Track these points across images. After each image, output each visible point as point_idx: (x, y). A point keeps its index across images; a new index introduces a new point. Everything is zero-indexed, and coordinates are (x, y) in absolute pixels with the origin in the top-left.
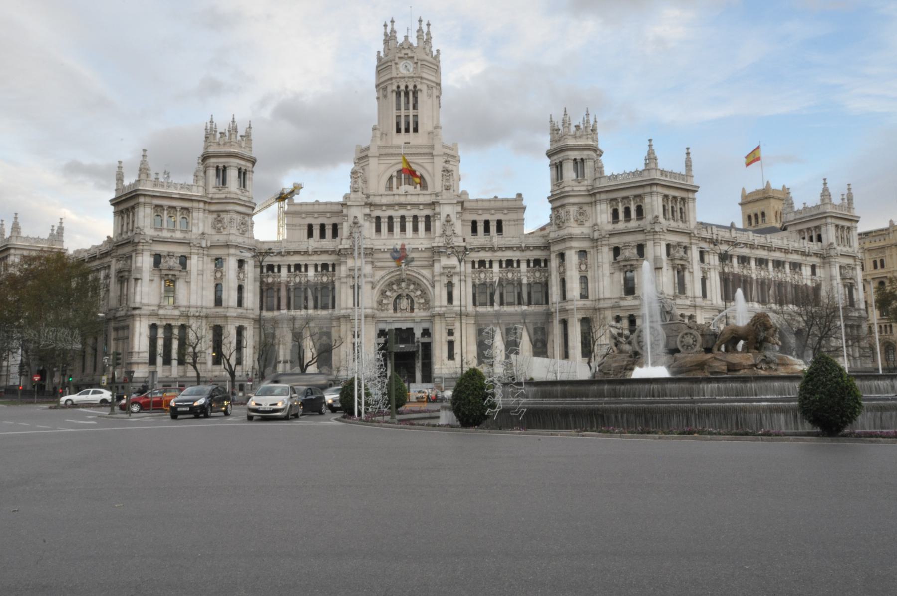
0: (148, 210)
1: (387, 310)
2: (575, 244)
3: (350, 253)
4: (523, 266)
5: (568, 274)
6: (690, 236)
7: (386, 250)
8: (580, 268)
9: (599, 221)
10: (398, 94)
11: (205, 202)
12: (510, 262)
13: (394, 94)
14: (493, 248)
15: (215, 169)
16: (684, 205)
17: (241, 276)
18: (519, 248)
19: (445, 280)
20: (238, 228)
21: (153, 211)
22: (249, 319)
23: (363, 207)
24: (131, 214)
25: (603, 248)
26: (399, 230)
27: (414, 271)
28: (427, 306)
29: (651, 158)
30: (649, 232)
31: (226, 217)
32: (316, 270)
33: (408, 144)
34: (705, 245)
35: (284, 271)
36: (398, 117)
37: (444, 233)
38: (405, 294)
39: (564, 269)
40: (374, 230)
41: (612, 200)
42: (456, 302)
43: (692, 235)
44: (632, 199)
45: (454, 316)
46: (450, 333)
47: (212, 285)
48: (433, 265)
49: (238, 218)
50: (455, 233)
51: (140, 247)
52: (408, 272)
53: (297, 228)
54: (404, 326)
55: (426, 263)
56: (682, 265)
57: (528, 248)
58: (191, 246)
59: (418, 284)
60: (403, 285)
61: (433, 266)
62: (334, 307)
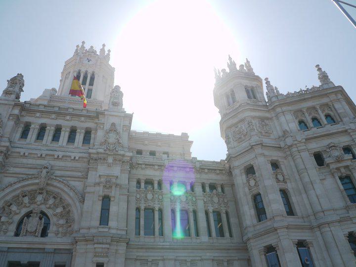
1: (5, 233)
7: (26, 154)
8: (277, 178)
19: (101, 191)
23: (11, 107)
25: (301, 154)
28: (69, 229)
29: (324, 77)
40: (18, 135)
42: (112, 223)
45: (109, 241)
52: (49, 182)
55: (79, 174)
59: (61, 198)
60: (39, 198)
61: (87, 178)
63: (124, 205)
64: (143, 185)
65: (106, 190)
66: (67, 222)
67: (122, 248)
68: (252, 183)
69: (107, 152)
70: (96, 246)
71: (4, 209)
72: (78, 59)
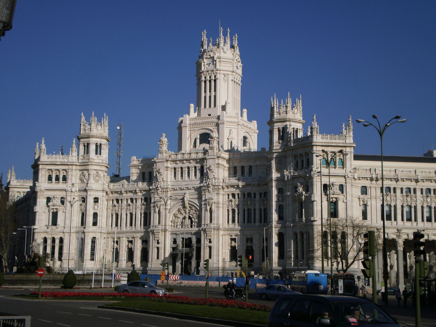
4: (258, 197)
6: (345, 178)
10: (205, 82)
11: (76, 165)
12: (249, 194)
17: (96, 207)
18: (254, 185)
20: (94, 179)
27: (191, 201)
34: (367, 183)
35: (125, 202)
36: (205, 97)
38: (187, 216)
43: (346, 177)
46: (210, 242)
49: (95, 172)
51: (39, 194)
54: (186, 236)
56: (336, 198)
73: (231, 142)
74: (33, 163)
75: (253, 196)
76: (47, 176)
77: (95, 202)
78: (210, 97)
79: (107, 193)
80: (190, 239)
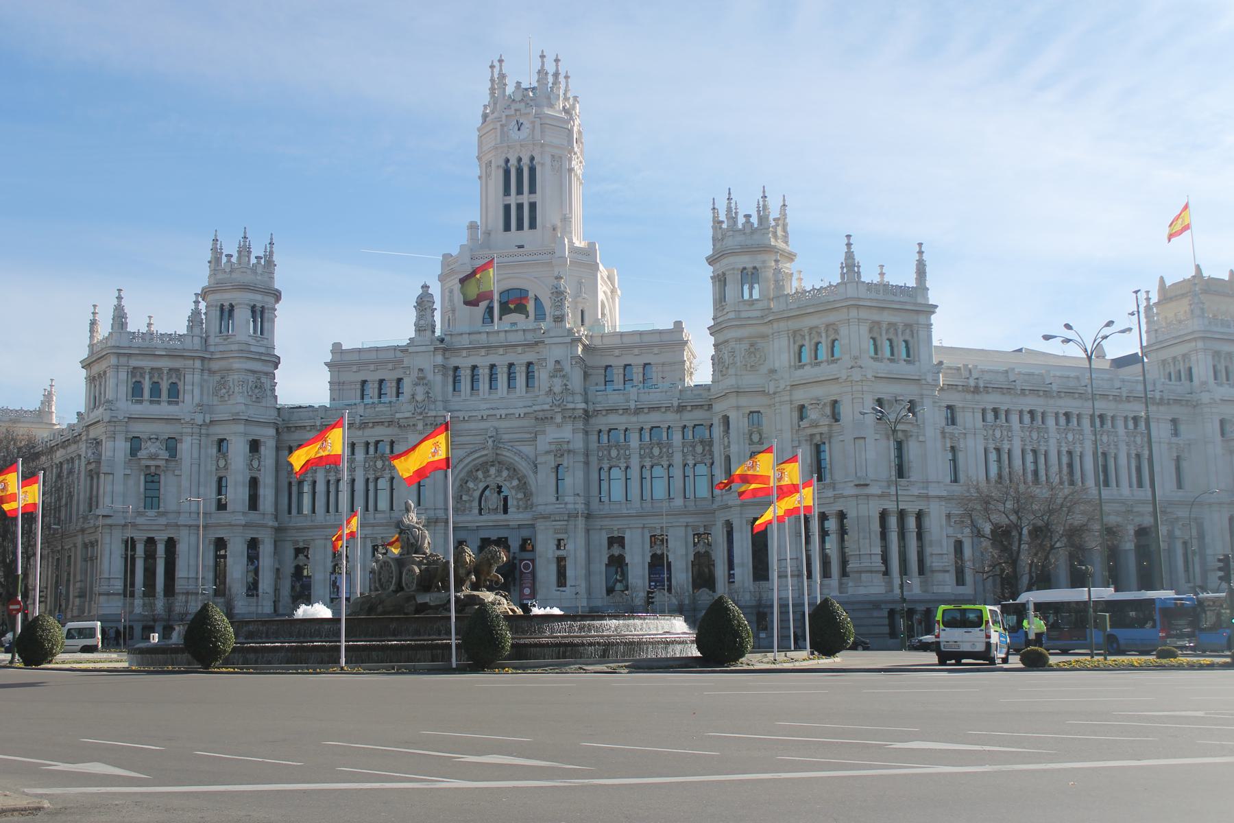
0: (123, 375)
1: (470, 511)
2: (744, 401)
3: (411, 424)
5: (734, 449)
9: (777, 365)
10: (507, 173)
11: (203, 359)
13: (501, 173)
14: (630, 409)
15: (218, 309)
16: (913, 337)
17: (255, 463)
19: (551, 461)
20: (250, 394)
21: (130, 376)
22: (266, 527)
23: (432, 353)
24: (103, 380)
26: (487, 386)
28: (529, 502)
29: (850, 266)
30: (846, 381)
31: (233, 378)
32: (367, 453)
33: (521, 249)
36: (507, 208)
37: (550, 390)
38: (493, 486)
39: (729, 442)
40: (450, 388)
41: (795, 332)
42: (567, 499)
43: (923, 382)
44: (823, 329)
45: (566, 518)
47: (215, 479)
48: (535, 439)
49: (251, 378)
50: (567, 389)
52: (498, 452)
53: (345, 387)
54: (494, 535)
55: (529, 436)
57: (681, 409)
58: (182, 423)
59: (514, 469)
60: (493, 471)
62: (392, 509)
63: (580, 475)
64: (604, 438)
65: (558, 459)
66: (525, 496)
67: (581, 522)
68: (726, 439)
69: (553, 408)
70: (554, 523)
71: (462, 487)
72: (499, 127)
73: (582, 312)
74: (84, 354)
75: (665, 434)
76: (130, 385)
77: (250, 452)
78: (520, 207)
79: (277, 430)
80: (502, 542)
